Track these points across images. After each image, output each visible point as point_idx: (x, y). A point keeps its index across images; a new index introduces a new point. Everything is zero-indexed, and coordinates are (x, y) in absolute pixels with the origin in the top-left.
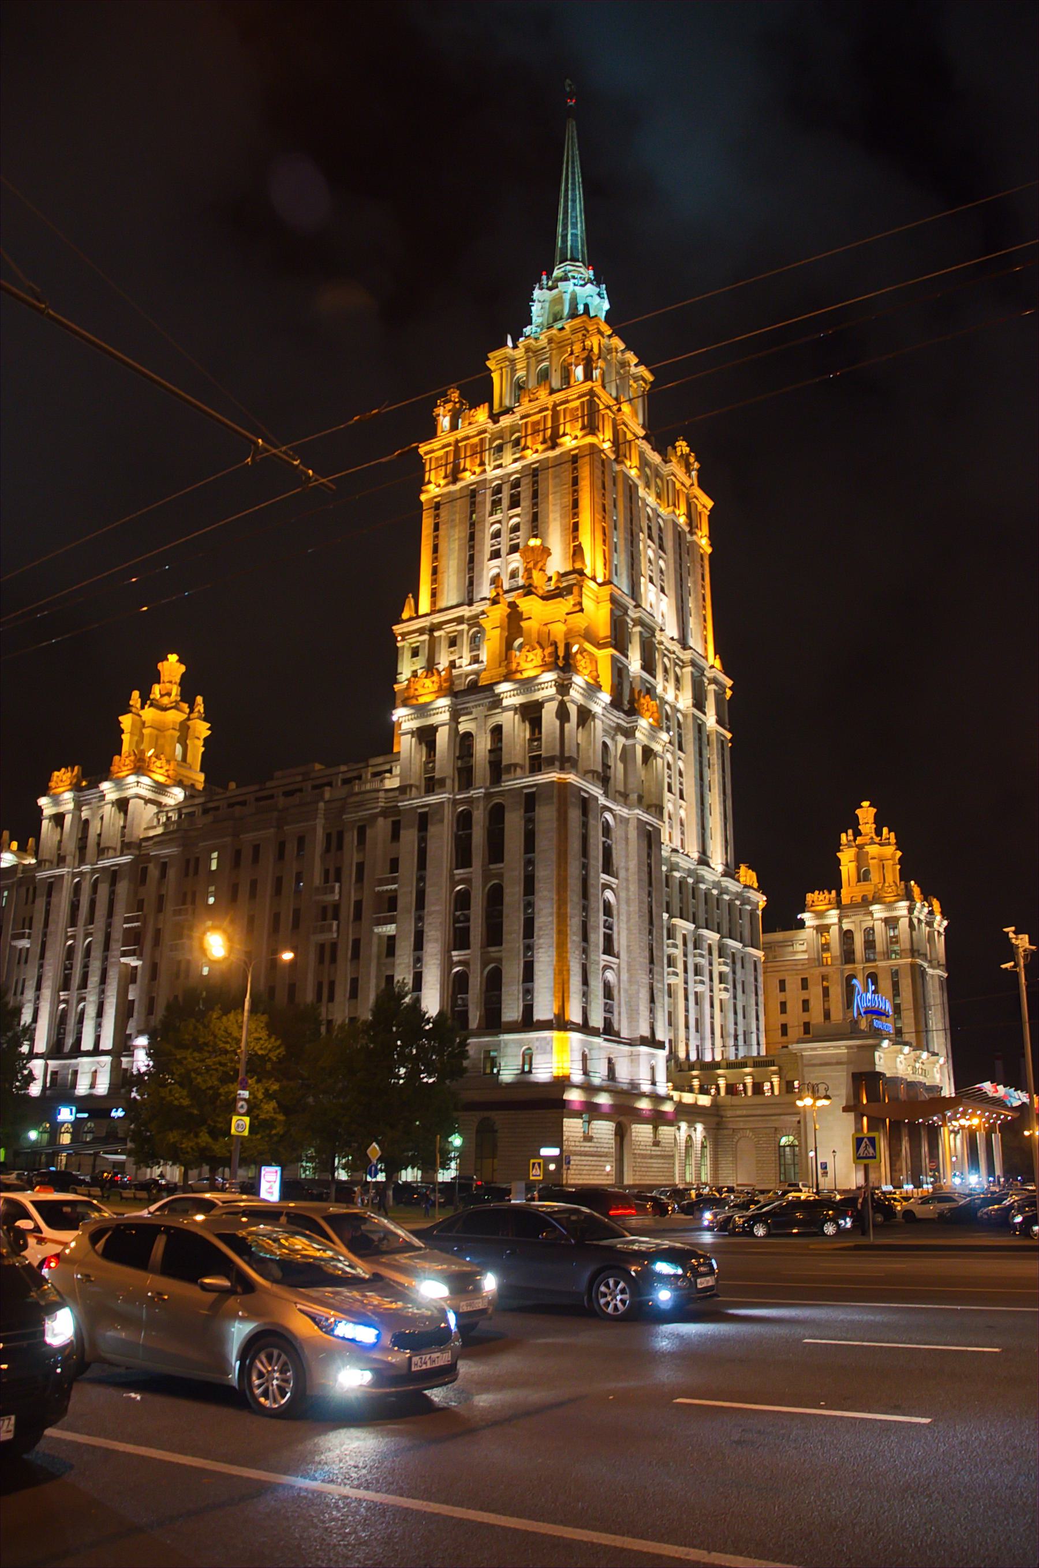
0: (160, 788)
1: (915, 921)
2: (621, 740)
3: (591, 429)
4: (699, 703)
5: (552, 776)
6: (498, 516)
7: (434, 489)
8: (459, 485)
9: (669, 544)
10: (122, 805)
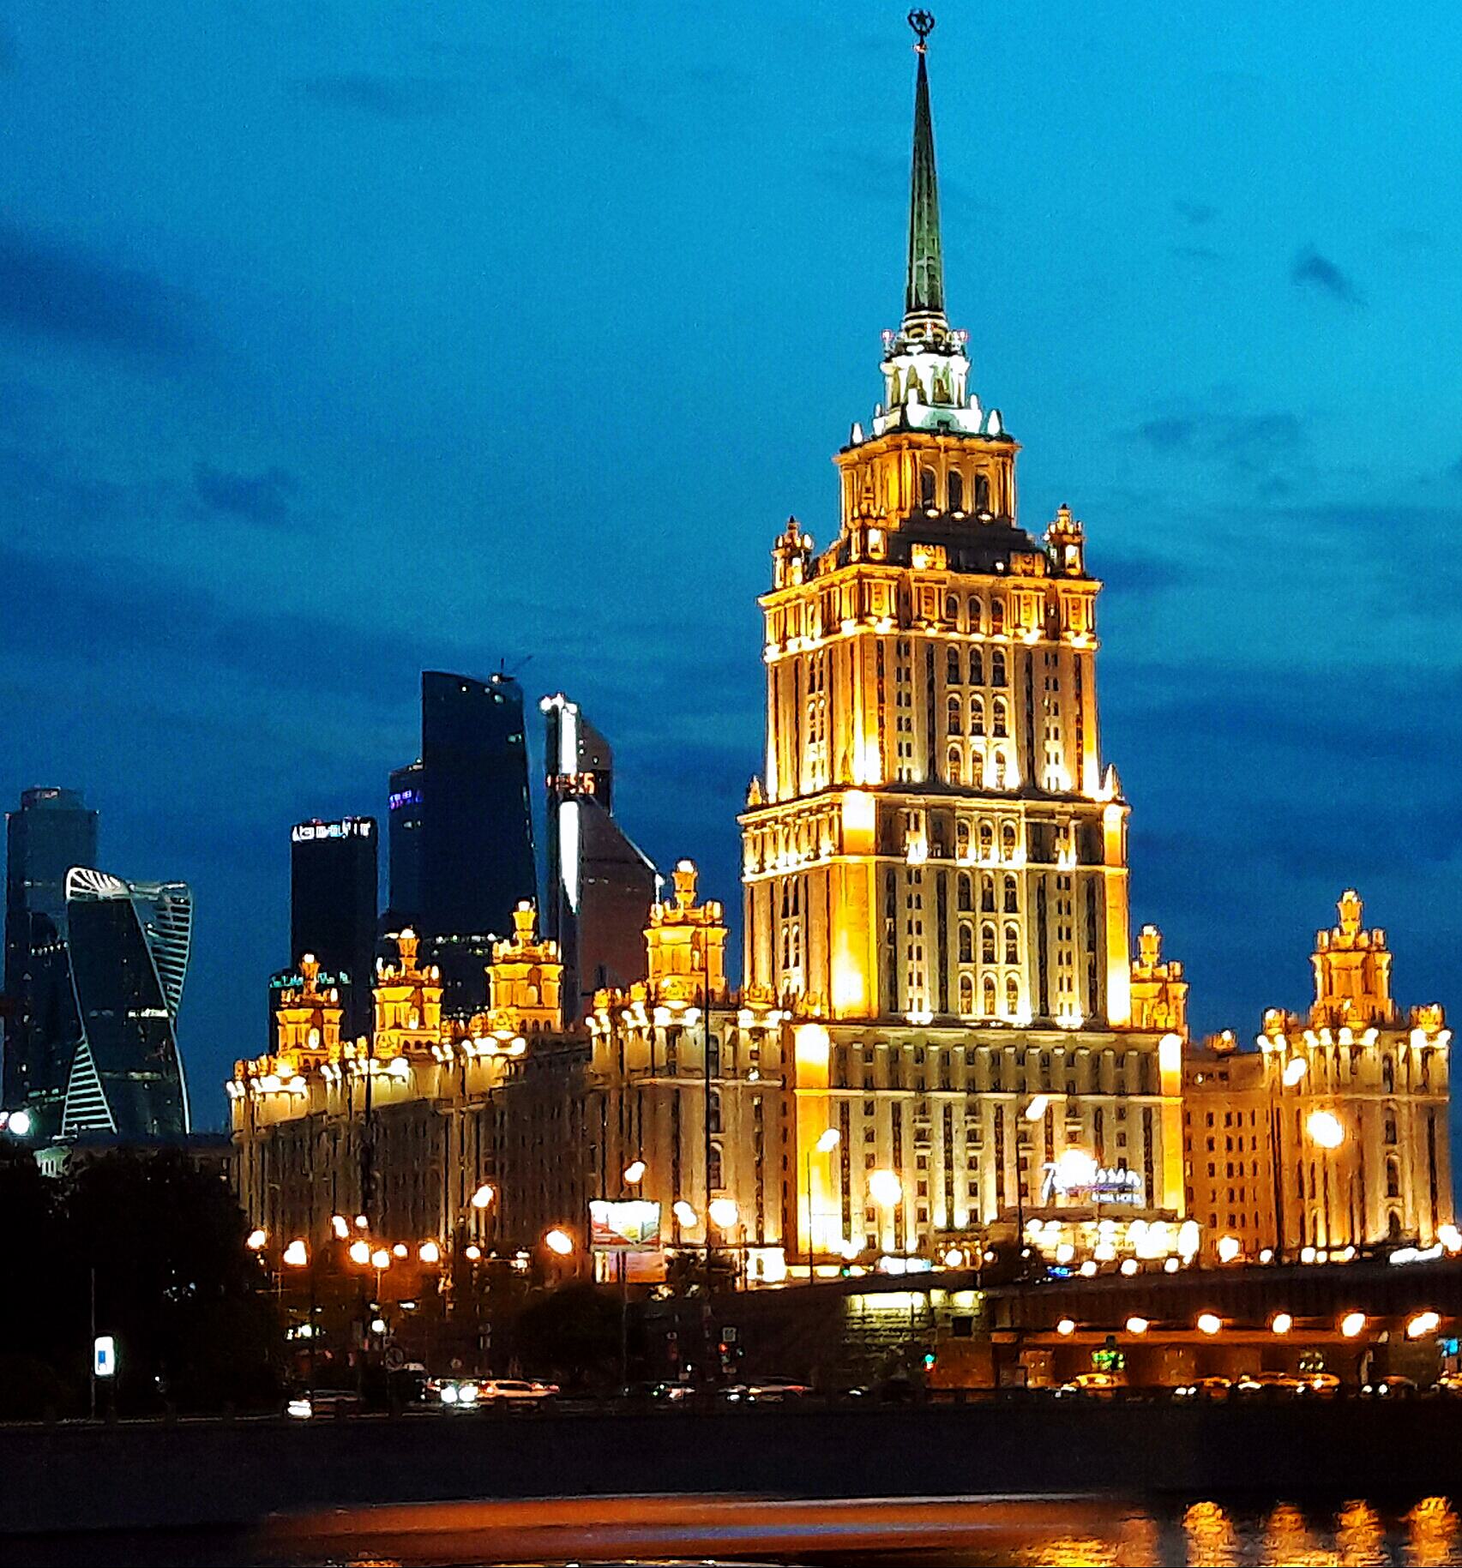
1: (1345, 1053)
2: (729, 1030)
3: (862, 616)
4: (1041, 850)
5: (646, 1081)
6: (813, 696)
7: (772, 654)
8: (786, 654)
9: (1009, 675)
10: (477, 1058)
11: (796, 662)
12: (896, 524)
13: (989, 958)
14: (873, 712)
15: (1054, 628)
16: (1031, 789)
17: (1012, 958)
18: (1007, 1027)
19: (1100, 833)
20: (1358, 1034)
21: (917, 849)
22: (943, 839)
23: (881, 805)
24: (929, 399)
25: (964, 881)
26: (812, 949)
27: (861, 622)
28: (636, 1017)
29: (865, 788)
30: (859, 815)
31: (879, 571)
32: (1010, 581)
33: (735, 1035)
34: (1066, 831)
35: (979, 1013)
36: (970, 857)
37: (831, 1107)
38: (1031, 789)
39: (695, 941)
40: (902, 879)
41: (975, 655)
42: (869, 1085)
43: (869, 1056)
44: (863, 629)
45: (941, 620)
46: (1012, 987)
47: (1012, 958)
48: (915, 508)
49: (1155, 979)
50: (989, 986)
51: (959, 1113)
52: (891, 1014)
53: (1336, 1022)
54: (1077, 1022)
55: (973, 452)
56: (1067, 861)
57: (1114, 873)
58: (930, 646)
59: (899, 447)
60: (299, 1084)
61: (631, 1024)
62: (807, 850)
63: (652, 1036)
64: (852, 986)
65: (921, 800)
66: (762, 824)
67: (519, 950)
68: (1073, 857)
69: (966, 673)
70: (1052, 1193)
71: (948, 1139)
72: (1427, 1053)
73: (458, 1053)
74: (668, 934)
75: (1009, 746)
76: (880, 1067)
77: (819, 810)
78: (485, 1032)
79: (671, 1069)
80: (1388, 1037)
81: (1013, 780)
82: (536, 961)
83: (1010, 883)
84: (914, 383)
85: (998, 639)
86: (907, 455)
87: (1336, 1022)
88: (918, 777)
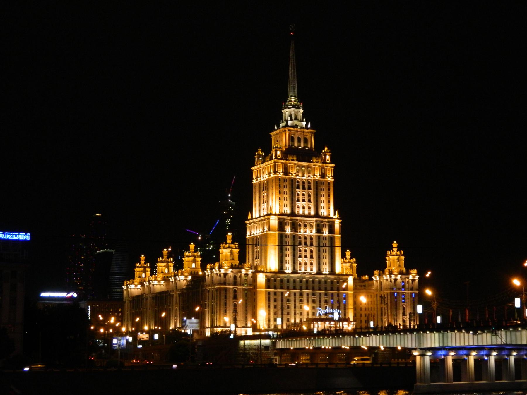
0: (186, 277)
2: (239, 274)
3: (275, 172)
4: (319, 231)
5: (219, 287)
7: (254, 181)
9: (312, 187)
11: (260, 183)
12: (284, 149)
13: (306, 257)
14: (278, 196)
15: (323, 176)
16: (317, 215)
17: (312, 257)
18: (310, 274)
19: (334, 226)
20: (396, 276)
21: (288, 230)
22: (295, 227)
23: (279, 219)
24: (293, 119)
25: (300, 238)
26: (262, 256)
27: (275, 174)
28: (216, 271)
29: (275, 215)
30: (274, 221)
31: (280, 161)
32: (312, 164)
33: (241, 276)
34: (326, 225)
35: (303, 270)
36: (302, 232)
37: (266, 294)
38: (317, 215)
39: (231, 252)
40: (284, 237)
41: (303, 182)
42: (275, 288)
43: (275, 281)
44: (276, 175)
45: (295, 173)
46: (311, 264)
47: (312, 257)
48: (289, 146)
49: (349, 262)
50: (306, 264)
51: (298, 295)
52: (281, 270)
53: (391, 273)
54: (327, 273)
55: (304, 132)
56: (326, 233)
57: (338, 236)
58: (292, 180)
59: (285, 131)
60: (139, 286)
61: (215, 272)
62: (261, 230)
63: (220, 275)
64: (272, 264)
65: (289, 218)
66: (251, 223)
67: (190, 254)
68: (327, 232)
69: (301, 187)
70: (320, 315)
71: (295, 301)
72: (413, 280)
73: (175, 279)
74: (225, 251)
75: (312, 205)
76: (278, 284)
77: (264, 220)
78: (182, 274)
79: (225, 284)
80: (404, 277)
81: (312, 213)
82: (195, 257)
83: (311, 238)
84: (290, 116)
85: (309, 178)
86: (287, 133)
87: (391, 273)
88: (289, 212)
